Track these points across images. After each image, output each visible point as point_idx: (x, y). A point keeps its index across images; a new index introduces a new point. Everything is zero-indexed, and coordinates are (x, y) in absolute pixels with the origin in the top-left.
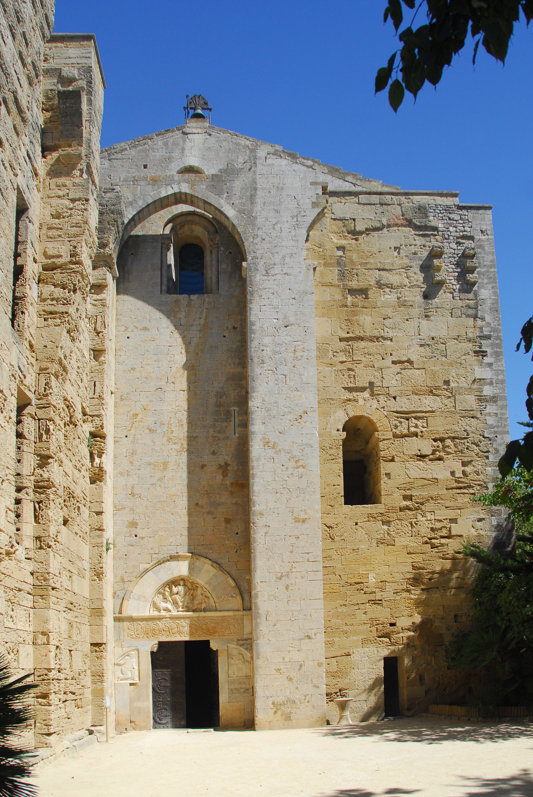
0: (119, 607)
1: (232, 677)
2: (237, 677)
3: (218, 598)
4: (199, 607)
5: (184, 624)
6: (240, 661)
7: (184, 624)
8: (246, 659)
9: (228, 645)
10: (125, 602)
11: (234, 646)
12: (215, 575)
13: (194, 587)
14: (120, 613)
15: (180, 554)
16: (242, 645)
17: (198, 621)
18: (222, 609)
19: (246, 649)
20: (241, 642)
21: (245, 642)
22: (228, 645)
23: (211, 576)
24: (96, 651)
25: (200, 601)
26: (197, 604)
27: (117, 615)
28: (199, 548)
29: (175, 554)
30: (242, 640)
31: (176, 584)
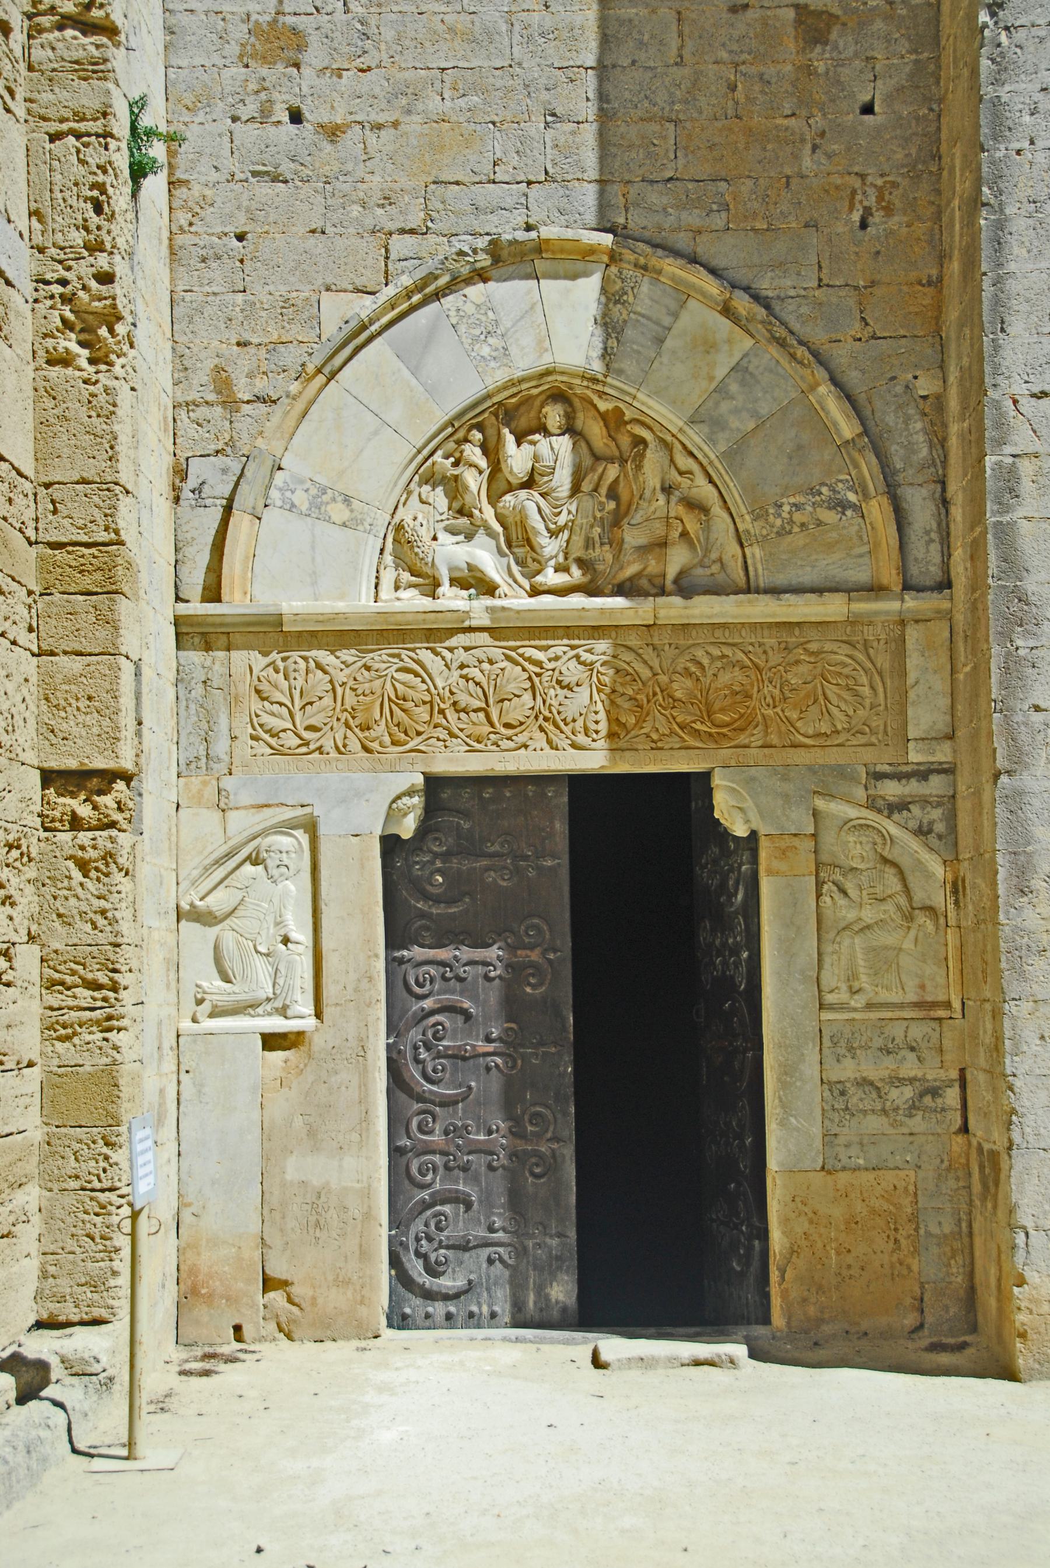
0: (203, 558)
1: (841, 1007)
2: (870, 1006)
3: (760, 514)
4: (653, 566)
5: (572, 671)
6: (889, 907)
7: (572, 671)
8: (919, 896)
9: (820, 803)
10: (241, 524)
11: (852, 812)
13: (625, 441)
14: (213, 593)
15: (547, 232)
17: (648, 654)
18: (781, 579)
19: (922, 832)
20: (892, 790)
21: (913, 787)
22: (820, 803)
23: (720, 372)
24: (76, 823)
25: (659, 529)
26: (643, 550)
27: (196, 608)
28: (655, 197)
29: (521, 235)
30: (899, 777)
31: (523, 422)
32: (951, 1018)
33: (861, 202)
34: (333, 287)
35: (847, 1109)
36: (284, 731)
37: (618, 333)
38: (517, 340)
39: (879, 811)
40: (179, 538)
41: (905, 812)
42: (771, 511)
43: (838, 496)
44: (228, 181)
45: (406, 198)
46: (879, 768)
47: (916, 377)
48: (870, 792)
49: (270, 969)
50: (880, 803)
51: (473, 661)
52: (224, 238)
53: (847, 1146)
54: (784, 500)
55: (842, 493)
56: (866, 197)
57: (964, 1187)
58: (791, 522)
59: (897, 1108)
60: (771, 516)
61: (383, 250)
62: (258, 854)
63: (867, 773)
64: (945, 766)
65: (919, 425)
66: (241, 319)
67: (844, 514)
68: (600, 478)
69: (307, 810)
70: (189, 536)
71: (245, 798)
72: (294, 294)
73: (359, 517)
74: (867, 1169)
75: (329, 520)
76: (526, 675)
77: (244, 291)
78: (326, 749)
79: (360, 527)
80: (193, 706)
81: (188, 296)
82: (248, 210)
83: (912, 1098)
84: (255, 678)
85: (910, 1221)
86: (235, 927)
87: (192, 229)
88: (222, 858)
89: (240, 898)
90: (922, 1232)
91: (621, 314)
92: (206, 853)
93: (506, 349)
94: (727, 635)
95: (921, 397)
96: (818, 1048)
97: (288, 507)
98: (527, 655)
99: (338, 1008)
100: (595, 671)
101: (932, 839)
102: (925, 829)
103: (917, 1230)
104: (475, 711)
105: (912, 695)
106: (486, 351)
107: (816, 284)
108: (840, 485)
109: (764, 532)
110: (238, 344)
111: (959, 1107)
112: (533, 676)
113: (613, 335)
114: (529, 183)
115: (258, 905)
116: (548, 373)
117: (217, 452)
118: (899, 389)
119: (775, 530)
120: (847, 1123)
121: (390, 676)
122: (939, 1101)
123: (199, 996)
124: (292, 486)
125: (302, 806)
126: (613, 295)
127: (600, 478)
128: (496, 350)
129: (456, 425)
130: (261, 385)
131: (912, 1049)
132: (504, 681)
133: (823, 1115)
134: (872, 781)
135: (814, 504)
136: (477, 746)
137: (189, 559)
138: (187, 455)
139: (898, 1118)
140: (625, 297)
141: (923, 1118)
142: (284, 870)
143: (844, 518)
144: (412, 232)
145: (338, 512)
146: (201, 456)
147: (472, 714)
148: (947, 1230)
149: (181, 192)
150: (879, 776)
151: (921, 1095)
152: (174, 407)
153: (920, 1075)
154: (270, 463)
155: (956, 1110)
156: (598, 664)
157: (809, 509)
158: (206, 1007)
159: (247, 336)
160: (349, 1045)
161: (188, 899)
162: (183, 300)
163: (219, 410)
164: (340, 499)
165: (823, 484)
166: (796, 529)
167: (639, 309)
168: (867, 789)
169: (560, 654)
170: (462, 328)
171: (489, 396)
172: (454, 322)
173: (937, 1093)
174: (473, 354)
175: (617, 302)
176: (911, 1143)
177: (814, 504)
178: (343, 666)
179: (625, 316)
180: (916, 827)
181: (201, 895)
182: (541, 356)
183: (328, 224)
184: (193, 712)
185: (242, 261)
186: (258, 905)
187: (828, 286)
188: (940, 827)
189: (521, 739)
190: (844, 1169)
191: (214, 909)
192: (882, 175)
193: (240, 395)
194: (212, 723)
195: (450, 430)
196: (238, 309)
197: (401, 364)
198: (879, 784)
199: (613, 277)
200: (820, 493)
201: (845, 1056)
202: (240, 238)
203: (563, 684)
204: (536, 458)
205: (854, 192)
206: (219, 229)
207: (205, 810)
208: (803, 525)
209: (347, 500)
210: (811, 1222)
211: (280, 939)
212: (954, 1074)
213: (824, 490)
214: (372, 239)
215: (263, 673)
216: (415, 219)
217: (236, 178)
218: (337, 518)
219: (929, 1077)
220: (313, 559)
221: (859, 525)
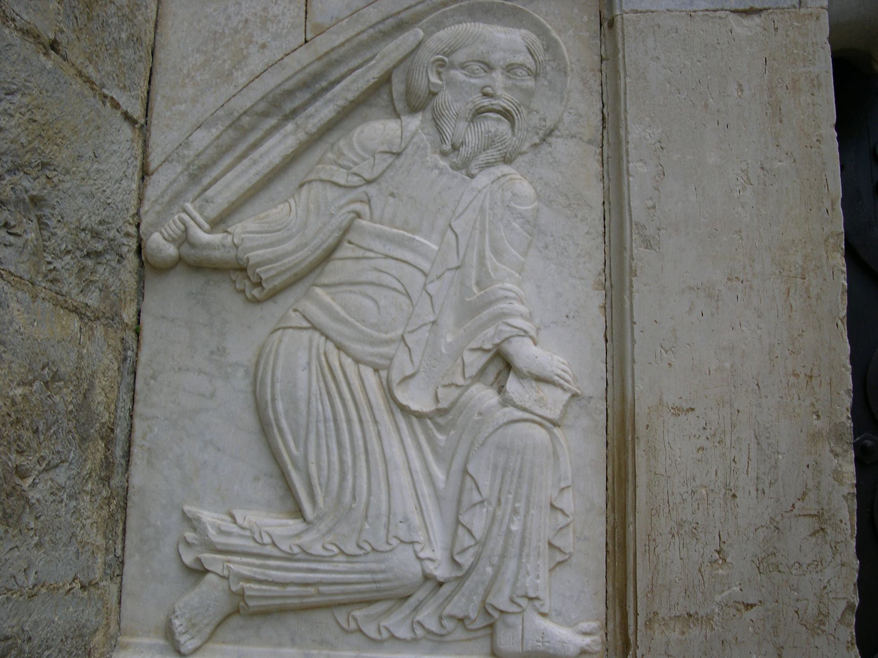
49: (439, 474)
86: (321, 318)
88: (290, 93)
89: (342, 218)
99: (695, 632)
115: (400, 242)
142: (495, 125)
161: (173, 226)
181: (213, 211)
186: (400, 242)
191: (255, 256)
211: (475, 361)
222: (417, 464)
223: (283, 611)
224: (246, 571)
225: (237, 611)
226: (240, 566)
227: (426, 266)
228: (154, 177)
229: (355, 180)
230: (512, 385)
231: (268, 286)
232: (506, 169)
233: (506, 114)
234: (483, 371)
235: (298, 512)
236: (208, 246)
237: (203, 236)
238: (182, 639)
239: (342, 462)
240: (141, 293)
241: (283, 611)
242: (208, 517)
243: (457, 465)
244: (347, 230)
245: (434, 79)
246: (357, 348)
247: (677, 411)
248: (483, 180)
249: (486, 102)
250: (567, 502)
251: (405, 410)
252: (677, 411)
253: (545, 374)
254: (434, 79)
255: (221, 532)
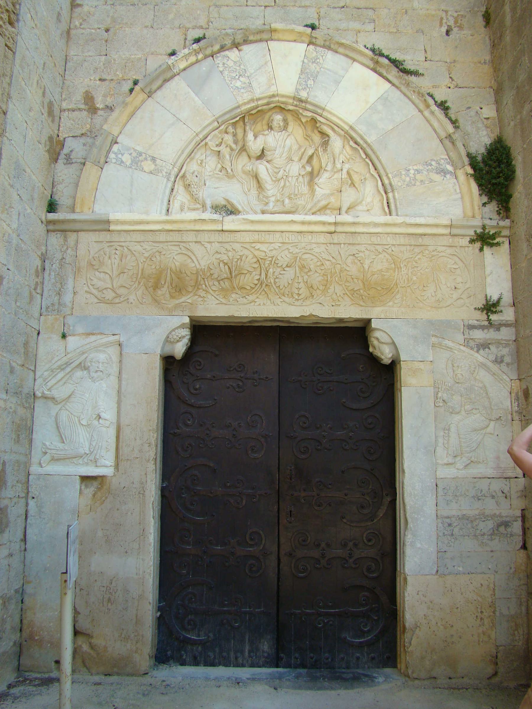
12: (384, 99)
16: (484, 346)
19: (498, 361)
20: (479, 335)
23: (372, 100)
32: (516, 478)
33: (446, 23)
34: (155, 53)
35: (452, 535)
36: (106, 288)
37: (314, 78)
38: (257, 79)
39: (472, 349)
40: (56, 180)
41: (487, 349)
42: (403, 173)
43: (441, 167)
44: (104, 5)
45: (198, 12)
46: (471, 322)
47: (481, 108)
48: (466, 337)
49: (88, 436)
50: (472, 343)
51: (223, 250)
52: (98, 30)
53: (452, 559)
54: (411, 167)
55: (444, 165)
56: (449, 21)
57: (524, 584)
58: (415, 179)
59: (484, 534)
60: (403, 176)
61: (184, 36)
62: (84, 364)
63: (464, 326)
64: (509, 323)
65: (485, 133)
66: (102, 68)
67: (445, 177)
68: (302, 155)
69: (116, 337)
70: (61, 179)
71: (80, 329)
72: (133, 56)
73: (160, 169)
74: (464, 574)
75: (142, 170)
76: (255, 260)
77: (106, 55)
78: (131, 300)
79: (160, 174)
80: (53, 274)
81: (75, 58)
82: (112, 17)
83: (493, 528)
84: (91, 257)
85: (490, 606)
87: (81, 27)
90: (497, 613)
91: (316, 68)
92: (53, 362)
93: (251, 84)
94: (379, 240)
95: (485, 118)
96: (435, 497)
97: (119, 162)
98: (256, 248)
100: (298, 258)
101: (504, 367)
102: (499, 360)
103: (494, 612)
104: (222, 280)
105: (488, 280)
106: (238, 84)
107: (424, 59)
108: (442, 161)
109: (400, 184)
110: (100, 80)
111: (521, 534)
112: (260, 260)
113: (311, 79)
114: (266, 7)
116: (273, 96)
117: (82, 134)
118: (473, 113)
119: (406, 183)
120: (452, 544)
121: (172, 258)
122: (509, 530)
123: (43, 450)
124: (122, 152)
125: (113, 335)
126: (311, 59)
127: (302, 155)
128: (245, 83)
129: (220, 121)
130: (109, 101)
131: (493, 497)
132: (242, 263)
133: (438, 539)
134: (467, 330)
135: (428, 170)
136: (223, 301)
137: (60, 191)
138: (64, 136)
139: (484, 541)
140: (318, 60)
141: (499, 541)
142: (99, 373)
143: (445, 178)
144: (201, 27)
145: (148, 166)
146: (73, 137)
147: (221, 282)
148: (513, 612)
149: (78, 10)
150: (471, 327)
151: (499, 525)
152: (61, 111)
153: (498, 513)
154: (110, 139)
155: (519, 536)
156: (300, 255)
157: (425, 172)
158: (48, 457)
159: (104, 77)
160: (134, 486)
161: (41, 391)
162: (72, 60)
163: (85, 113)
164: (149, 159)
165: (432, 160)
166: (418, 183)
167: (326, 66)
168: (464, 335)
169: (277, 247)
170: (226, 73)
171: (238, 107)
172: (221, 69)
173: (508, 525)
174: (231, 85)
175: (313, 62)
176: (492, 556)
177: (428, 170)
178: (144, 251)
179: (318, 69)
180: (494, 359)
181: (48, 388)
182: (270, 87)
183: (155, 24)
184: (53, 277)
185: (106, 41)
187: (431, 61)
188: (507, 359)
189: (250, 298)
190: (450, 574)
191: (56, 396)
192: (456, 12)
193: (98, 106)
194: (63, 283)
195: (216, 124)
196: (102, 64)
197: (190, 90)
198: (471, 332)
199: (311, 50)
200: (431, 165)
201: (451, 501)
202: (107, 31)
203: (279, 265)
204: (265, 143)
205: (442, 19)
206: (96, 26)
207: (55, 336)
208: (422, 181)
209: (154, 159)
210: (429, 608)
211: (94, 416)
212: (518, 513)
213: (433, 163)
214: (178, 30)
215: (97, 255)
216: (202, 22)
217: (108, 3)
218: (146, 169)
219: (503, 514)
220: (131, 191)
221: (454, 183)
222: (84, 434)
223: (61, 459)
224: (54, 452)
225: (52, 460)
226: (54, 452)
227: (86, 399)
228: (37, 380)
229: (74, 383)
230: (100, 420)
231: (58, 402)
232: (102, 381)
233: (101, 371)
234: (96, 418)
235: (64, 442)
236: (47, 394)
237: (46, 392)
238: (43, 464)
239: (71, 433)
240: (34, 403)
241: (61, 459)
242: (48, 443)
243: (91, 434)
244: (73, 392)
245: (89, 364)
246: (75, 414)
247: (128, 426)
248: (97, 384)
249: (98, 369)
250: (109, 440)
251: (82, 424)
252: (128, 426)
253: (106, 419)
254: (89, 364)
255: (49, 446)
